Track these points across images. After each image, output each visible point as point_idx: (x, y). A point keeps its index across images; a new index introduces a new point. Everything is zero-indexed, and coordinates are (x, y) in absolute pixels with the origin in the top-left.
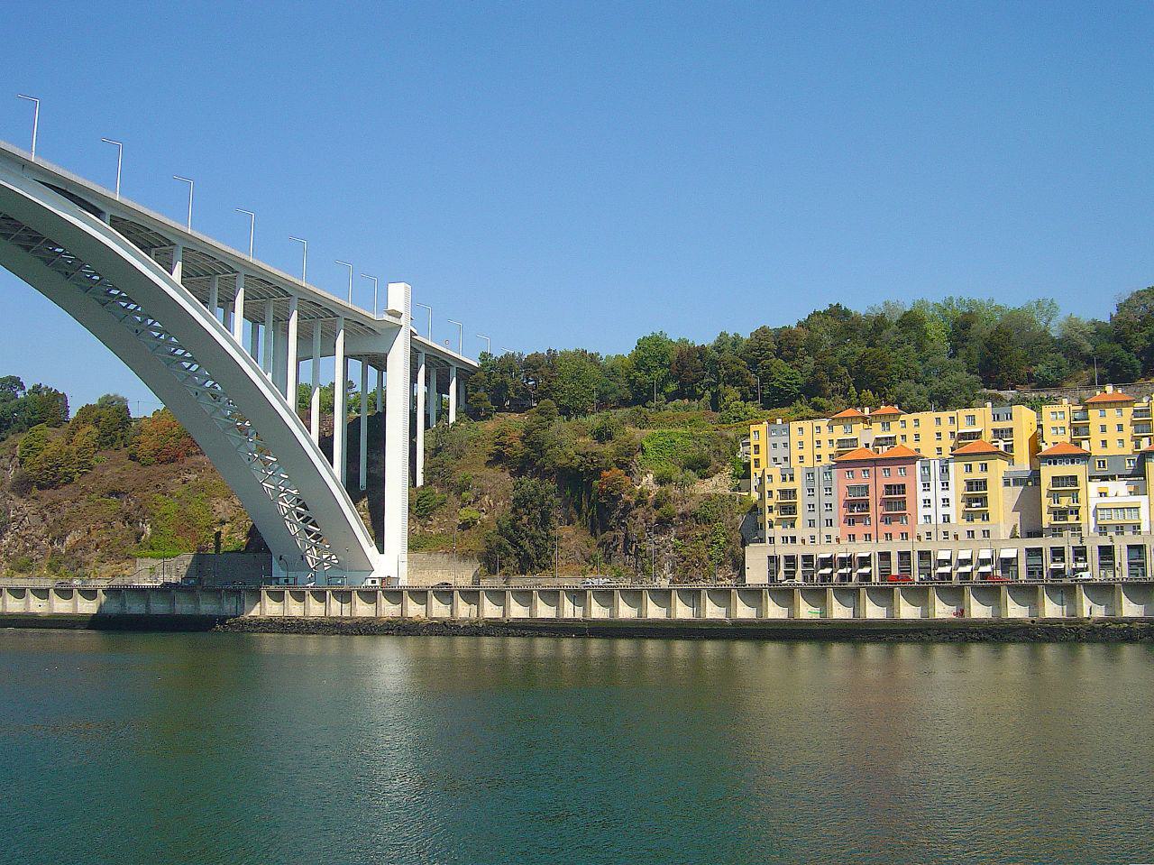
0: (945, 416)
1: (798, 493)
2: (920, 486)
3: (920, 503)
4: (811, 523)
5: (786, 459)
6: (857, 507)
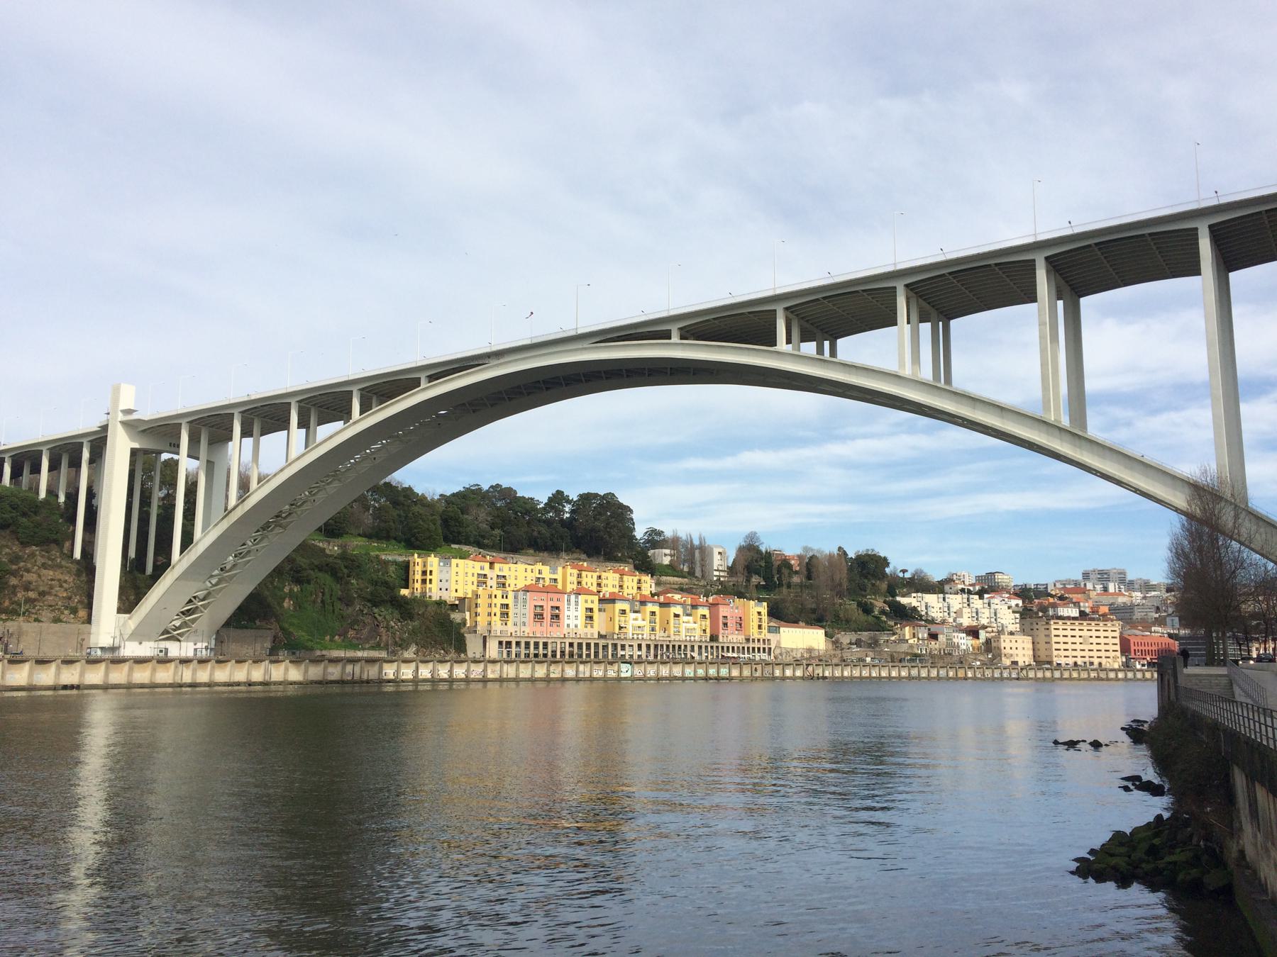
0: (529, 568)
1: (510, 606)
2: (566, 606)
3: (566, 618)
4: (515, 624)
5: (447, 581)
6: (539, 616)
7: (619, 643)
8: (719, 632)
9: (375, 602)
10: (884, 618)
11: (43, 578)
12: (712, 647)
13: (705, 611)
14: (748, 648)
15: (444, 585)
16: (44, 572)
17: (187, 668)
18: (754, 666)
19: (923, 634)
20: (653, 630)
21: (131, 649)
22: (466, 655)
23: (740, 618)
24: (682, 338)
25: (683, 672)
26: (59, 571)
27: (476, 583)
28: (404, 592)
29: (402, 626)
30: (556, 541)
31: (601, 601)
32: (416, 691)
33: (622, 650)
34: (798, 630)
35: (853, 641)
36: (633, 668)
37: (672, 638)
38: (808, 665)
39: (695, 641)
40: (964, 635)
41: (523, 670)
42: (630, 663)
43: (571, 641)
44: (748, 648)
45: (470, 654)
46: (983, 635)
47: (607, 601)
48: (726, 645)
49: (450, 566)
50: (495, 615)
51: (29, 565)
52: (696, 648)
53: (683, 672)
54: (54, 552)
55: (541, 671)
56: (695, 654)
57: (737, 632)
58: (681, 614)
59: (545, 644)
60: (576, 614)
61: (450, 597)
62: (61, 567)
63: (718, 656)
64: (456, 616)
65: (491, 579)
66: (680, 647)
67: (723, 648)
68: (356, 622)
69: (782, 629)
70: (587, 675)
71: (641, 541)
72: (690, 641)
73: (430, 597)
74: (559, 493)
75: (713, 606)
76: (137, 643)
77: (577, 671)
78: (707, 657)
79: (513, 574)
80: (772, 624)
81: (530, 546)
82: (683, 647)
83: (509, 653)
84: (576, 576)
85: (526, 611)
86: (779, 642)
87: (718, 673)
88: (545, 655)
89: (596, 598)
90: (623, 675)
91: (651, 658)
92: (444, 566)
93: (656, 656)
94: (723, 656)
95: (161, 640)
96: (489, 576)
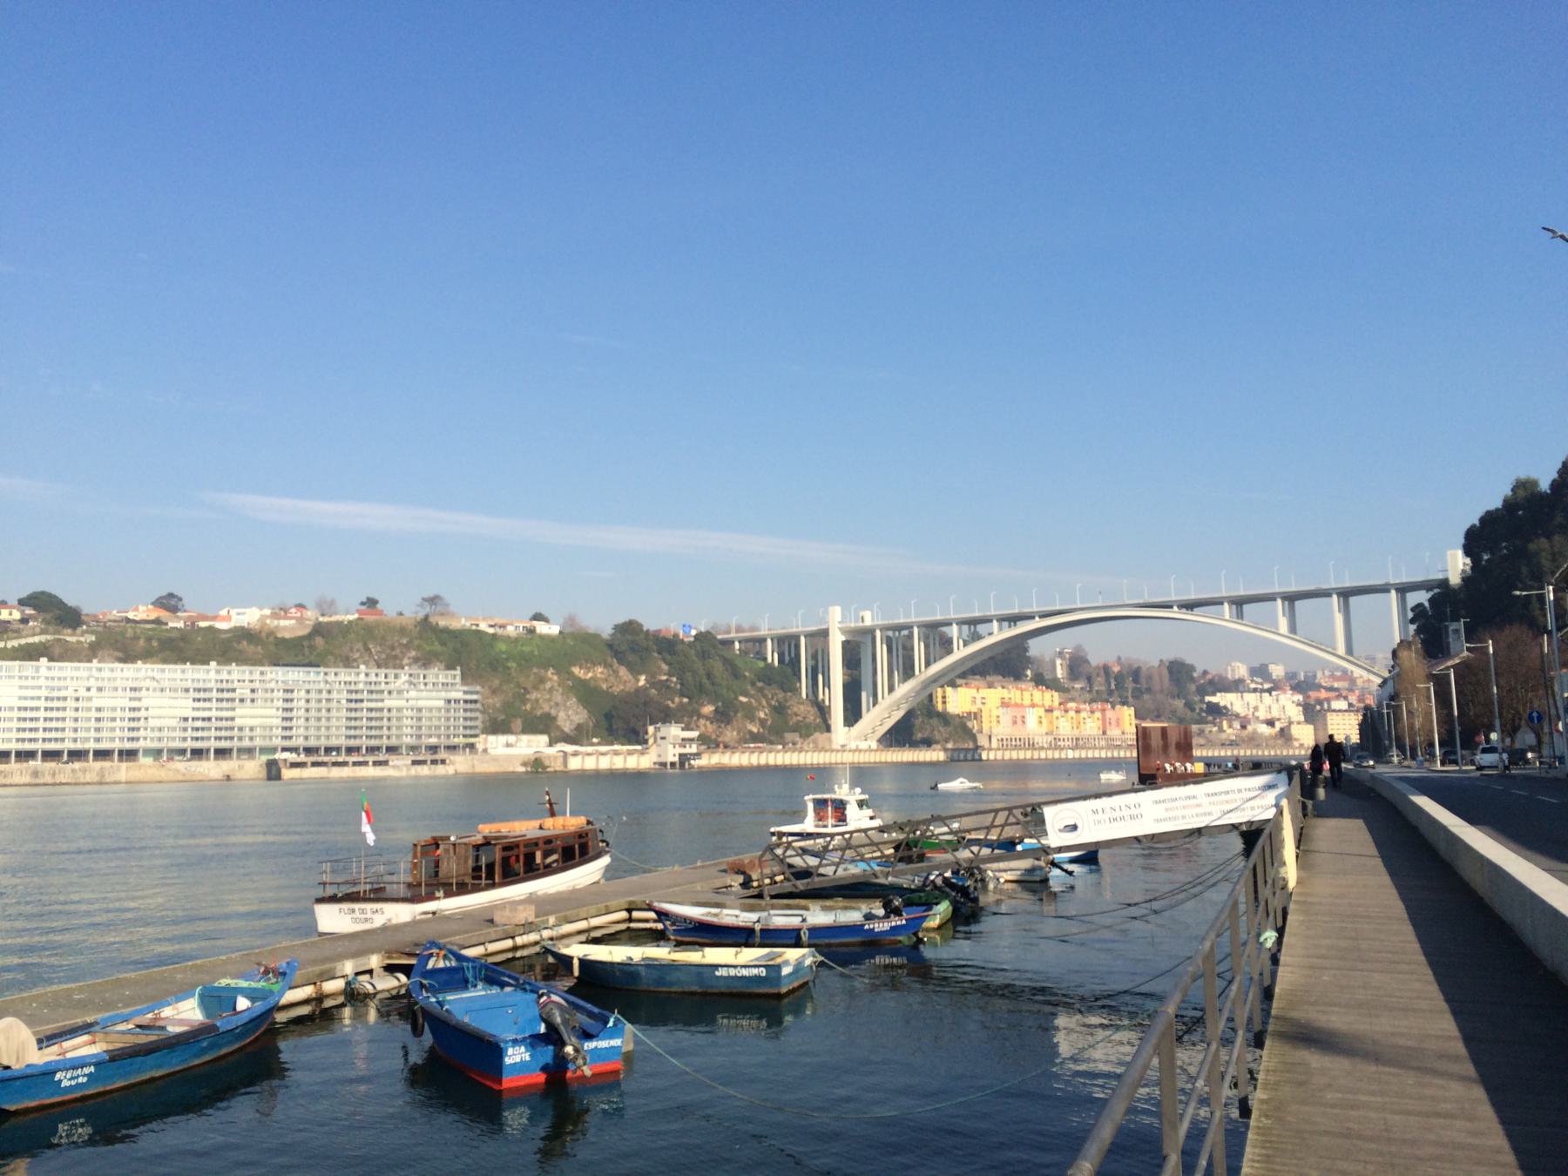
6: (1015, 722)
10: (1204, 714)
13: (1098, 714)
19: (1237, 725)
31: (1047, 711)
37: (1084, 733)
40: (1265, 726)
46: (1278, 725)
47: (1050, 710)
64: (969, 724)
75: (1103, 711)
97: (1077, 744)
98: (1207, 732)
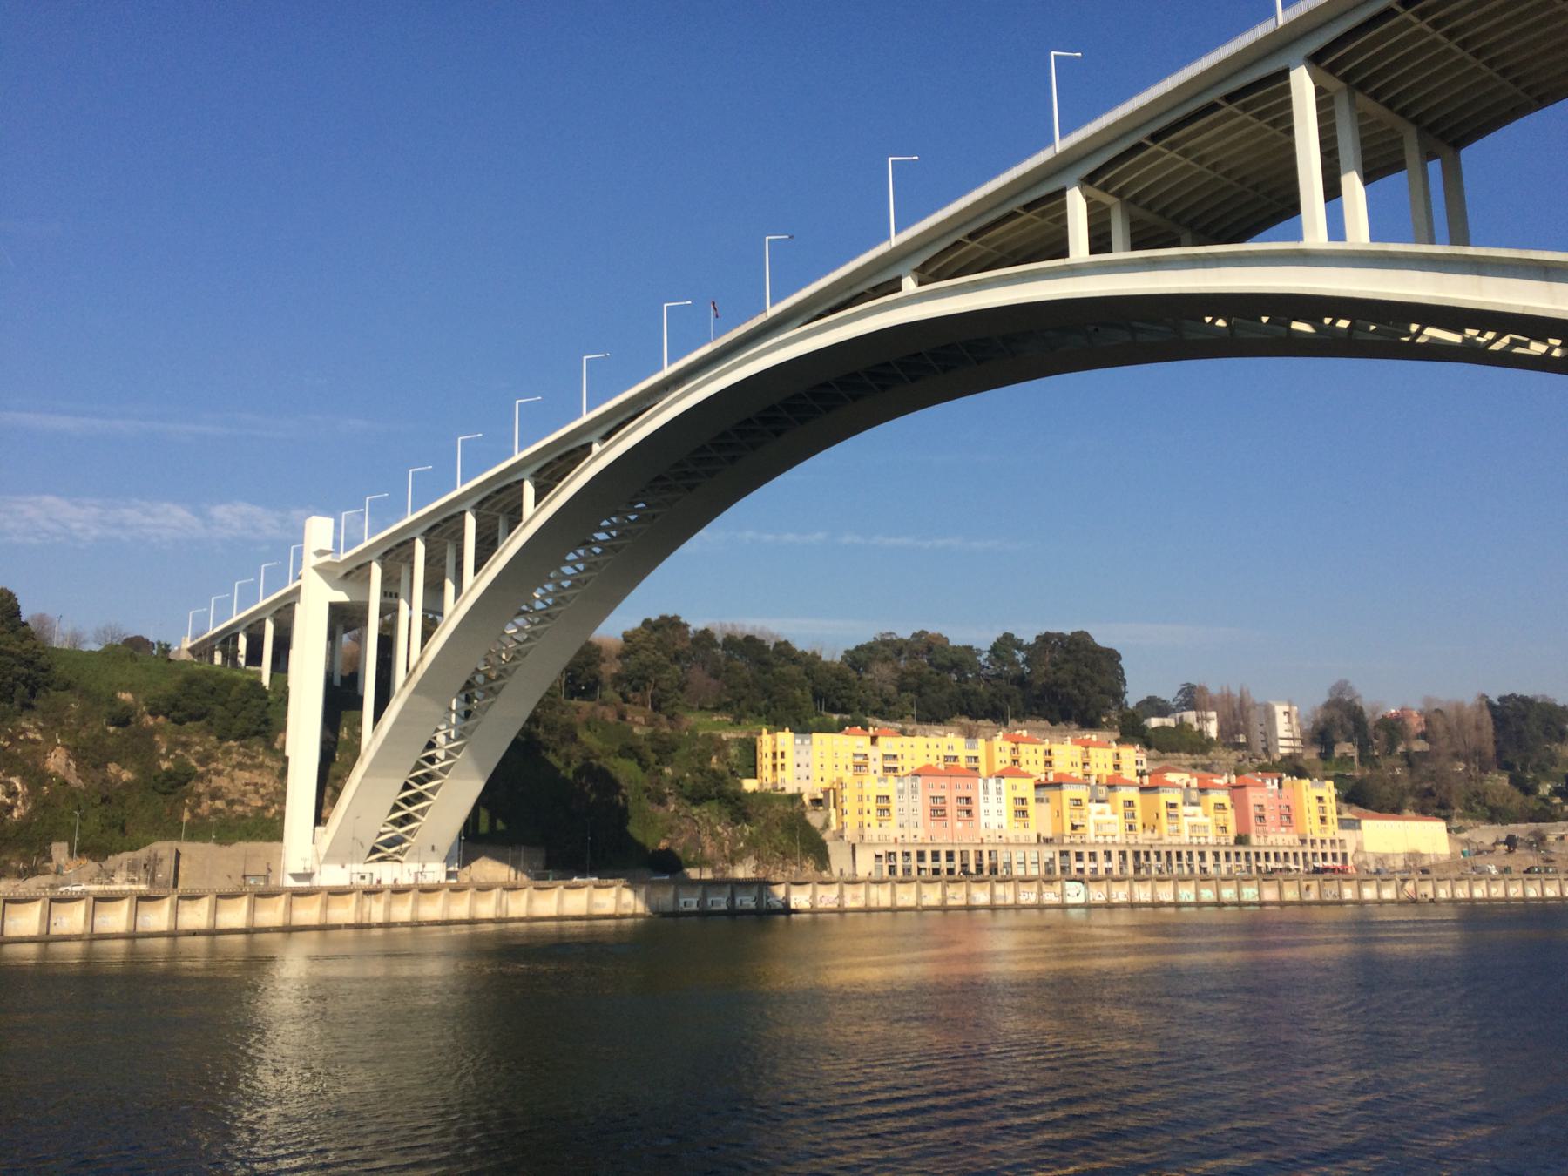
0: (933, 740)
1: (891, 798)
6: (938, 813)
7: (1073, 850)
8: (1249, 830)
9: (697, 798)
10: (1557, 800)
11: (236, 782)
12: (1237, 854)
13: (1223, 797)
14: (1305, 854)
15: (803, 771)
16: (237, 773)
17: (378, 900)
18: (1304, 884)
20: (1131, 827)
21: (332, 876)
22: (831, 872)
23: (1288, 806)
24: (920, 284)
25: (1176, 894)
26: (257, 772)
27: (851, 767)
28: (749, 785)
29: (734, 833)
30: (997, 702)
32: (814, 922)
33: (1077, 860)
34: (1400, 823)
35: (1503, 838)
36: (1087, 888)
37: (1167, 840)
38: (1405, 880)
39: (1207, 844)
41: (902, 895)
42: (1082, 881)
43: (991, 848)
44: (1305, 854)
45: (836, 872)
47: (1049, 786)
48: (1262, 851)
49: (811, 743)
50: (869, 812)
51: (221, 766)
52: (1209, 857)
53: (1176, 894)
54: (255, 748)
55: (932, 896)
56: (1209, 862)
57: (1283, 829)
58: (1180, 803)
59: (950, 856)
60: (1000, 807)
61: (810, 790)
62: (261, 766)
63: (1249, 869)
64: (815, 819)
65: (875, 760)
66: (1179, 855)
67: (1257, 854)
68: (671, 829)
69: (1364, 823)
70: (1010, 900)
71: (1175, 703)
72: (1106, 843)
73: (783, 789)
74: (1008, 637)
75: (1235, 790)
76: (339, 867)
77: (992, 895)
78: (1229, 869)
79: (907, 751)
80: (1346, 815)
81: (963, 713)
82: (1185, 856)
83: (892, 870)
84: (1008, 750)
85: (919, 806)
86: (1360, 844)
87: (1239, 896)
88: (950, 871)
89: (1030, 783)
90: (1070, 900)
91: (1130, 870)
92: (803, 743)
93: (1137, 869)
94: (1259, 868)
95: (371, 862)
96: (871, 757)
97: (1140, 863)
98: (1551, 839)
